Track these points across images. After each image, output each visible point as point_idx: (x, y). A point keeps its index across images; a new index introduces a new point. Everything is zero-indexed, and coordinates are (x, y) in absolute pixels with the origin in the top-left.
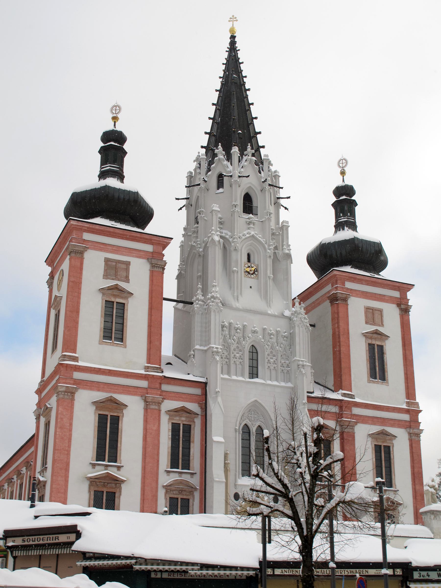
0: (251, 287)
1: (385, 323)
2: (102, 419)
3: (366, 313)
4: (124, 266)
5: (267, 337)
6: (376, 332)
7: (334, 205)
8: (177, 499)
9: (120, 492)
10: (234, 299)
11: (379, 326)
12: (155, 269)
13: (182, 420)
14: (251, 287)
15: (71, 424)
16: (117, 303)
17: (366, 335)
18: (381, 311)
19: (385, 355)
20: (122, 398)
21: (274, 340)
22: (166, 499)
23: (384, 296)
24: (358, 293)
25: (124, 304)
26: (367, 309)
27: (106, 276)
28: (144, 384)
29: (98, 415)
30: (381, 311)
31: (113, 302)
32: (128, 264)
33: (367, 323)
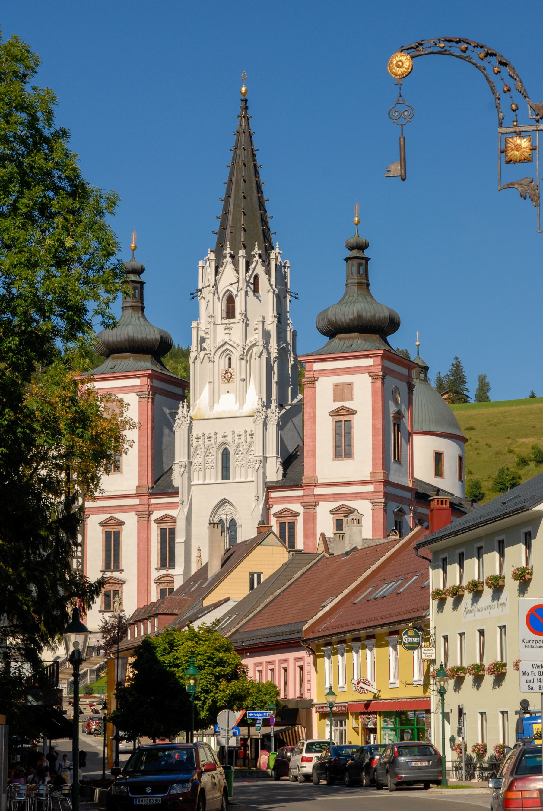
0: (228, 392)
1: (354, 397)
2: (107, 535)
3: (335, 391)
5: (236, 438)
6: (342, 408)
9: (122, 589)
11: (349, 400)
13: (167, 526)
17: (332, 414)
18: (351, 384)
19: (352, 430)
20: (120, 516)
22: (157, 591)
23: (354, 367)
24: (326, 372)
26: (336, 386)
28: (136, 501)
30: (351, 384)
33: (335, 401)
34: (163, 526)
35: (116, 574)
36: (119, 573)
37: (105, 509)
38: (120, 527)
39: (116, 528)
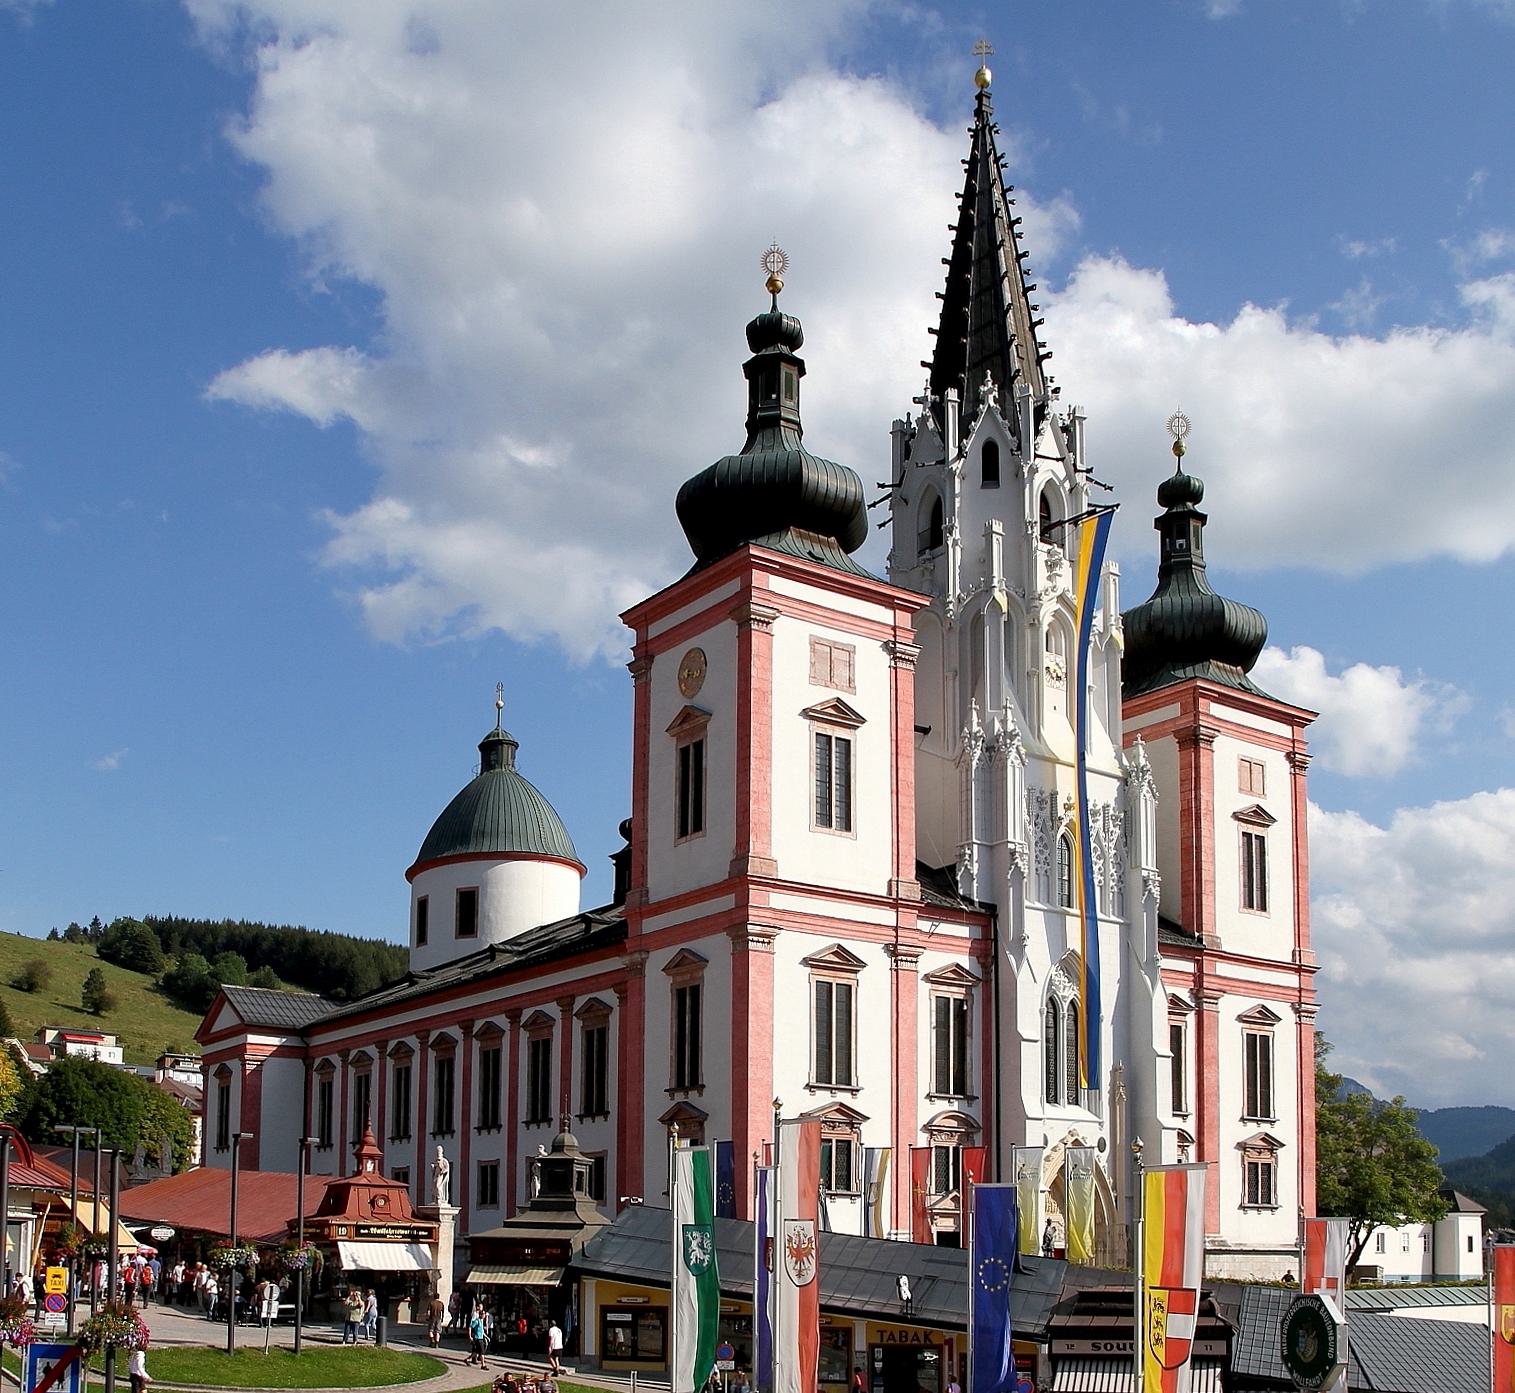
0: (1055, 708)
2: (824, 990)
4: (844, 656)
7: (1160, 523)
8: (948, 1148)
10: (1033, 734)
12: (899, 664)
14: (1055, 708)
15: (772, 1005)
16: (837, 738)
21: (1101, 823)
25: (849, 741)
27: (814, 679)
28: (888, 917)
29: (814, 985)
31: (830, 737)
32: (851, 651)
34: (945, 991)
35: (693, 1097)
36: (849, 1095)
37: (821, 922)
38: (852, 976)
39: (843, 978)
